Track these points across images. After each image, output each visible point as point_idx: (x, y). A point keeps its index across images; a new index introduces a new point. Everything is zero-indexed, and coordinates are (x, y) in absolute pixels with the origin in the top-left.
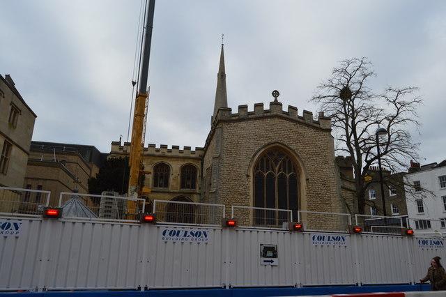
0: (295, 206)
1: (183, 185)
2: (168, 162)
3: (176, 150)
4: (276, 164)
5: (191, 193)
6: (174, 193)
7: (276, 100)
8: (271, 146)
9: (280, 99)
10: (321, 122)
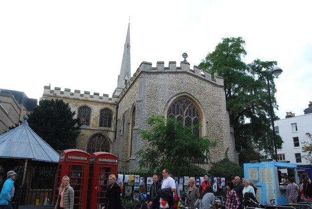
1: (101, 125)
2: (90, 105)
3: (96, 96)
4: (184, 110)
5: (108, 131)
8: (181, 95)
9: (188, 60)
10: (217, 79)
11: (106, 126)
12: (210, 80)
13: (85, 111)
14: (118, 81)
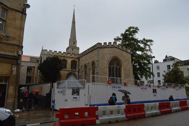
0: (120, 76)
1: (72, 68)
2: (66, 59)
5: (75, 71)
6: (69, 71)
13: (66, 61)
14: (69, 42)
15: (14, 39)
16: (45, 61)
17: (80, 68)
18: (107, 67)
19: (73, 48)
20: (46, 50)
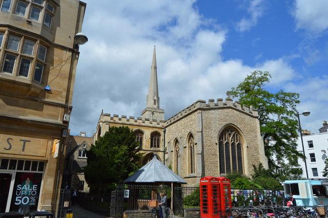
1: (151, 147)
2: (142, 129)
4: (230, 136)
7: (229, 97)
10: (253, 112)
11: (155, 147)
12: (248, 113)
13: (140, 132)
15: (59, 93)
16: (107, 134)
17: (166, 146)
18: (216, 144)
19: (153, 110)
20: (109, 115)
